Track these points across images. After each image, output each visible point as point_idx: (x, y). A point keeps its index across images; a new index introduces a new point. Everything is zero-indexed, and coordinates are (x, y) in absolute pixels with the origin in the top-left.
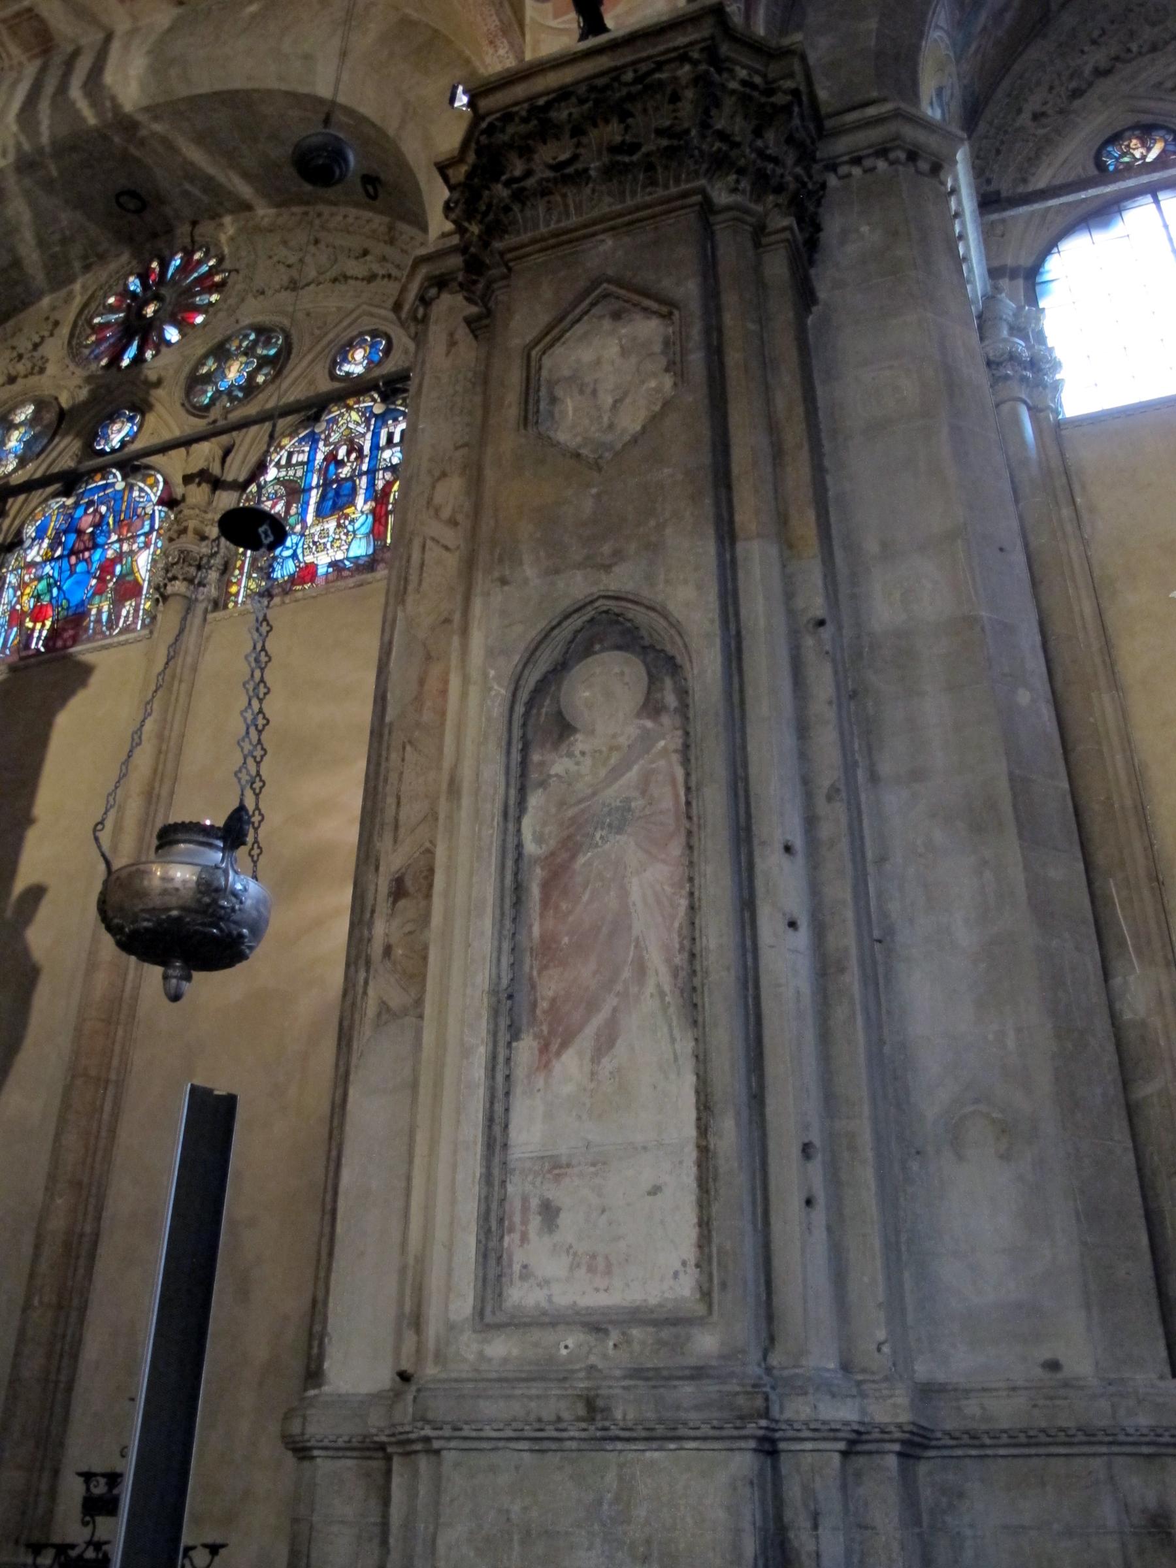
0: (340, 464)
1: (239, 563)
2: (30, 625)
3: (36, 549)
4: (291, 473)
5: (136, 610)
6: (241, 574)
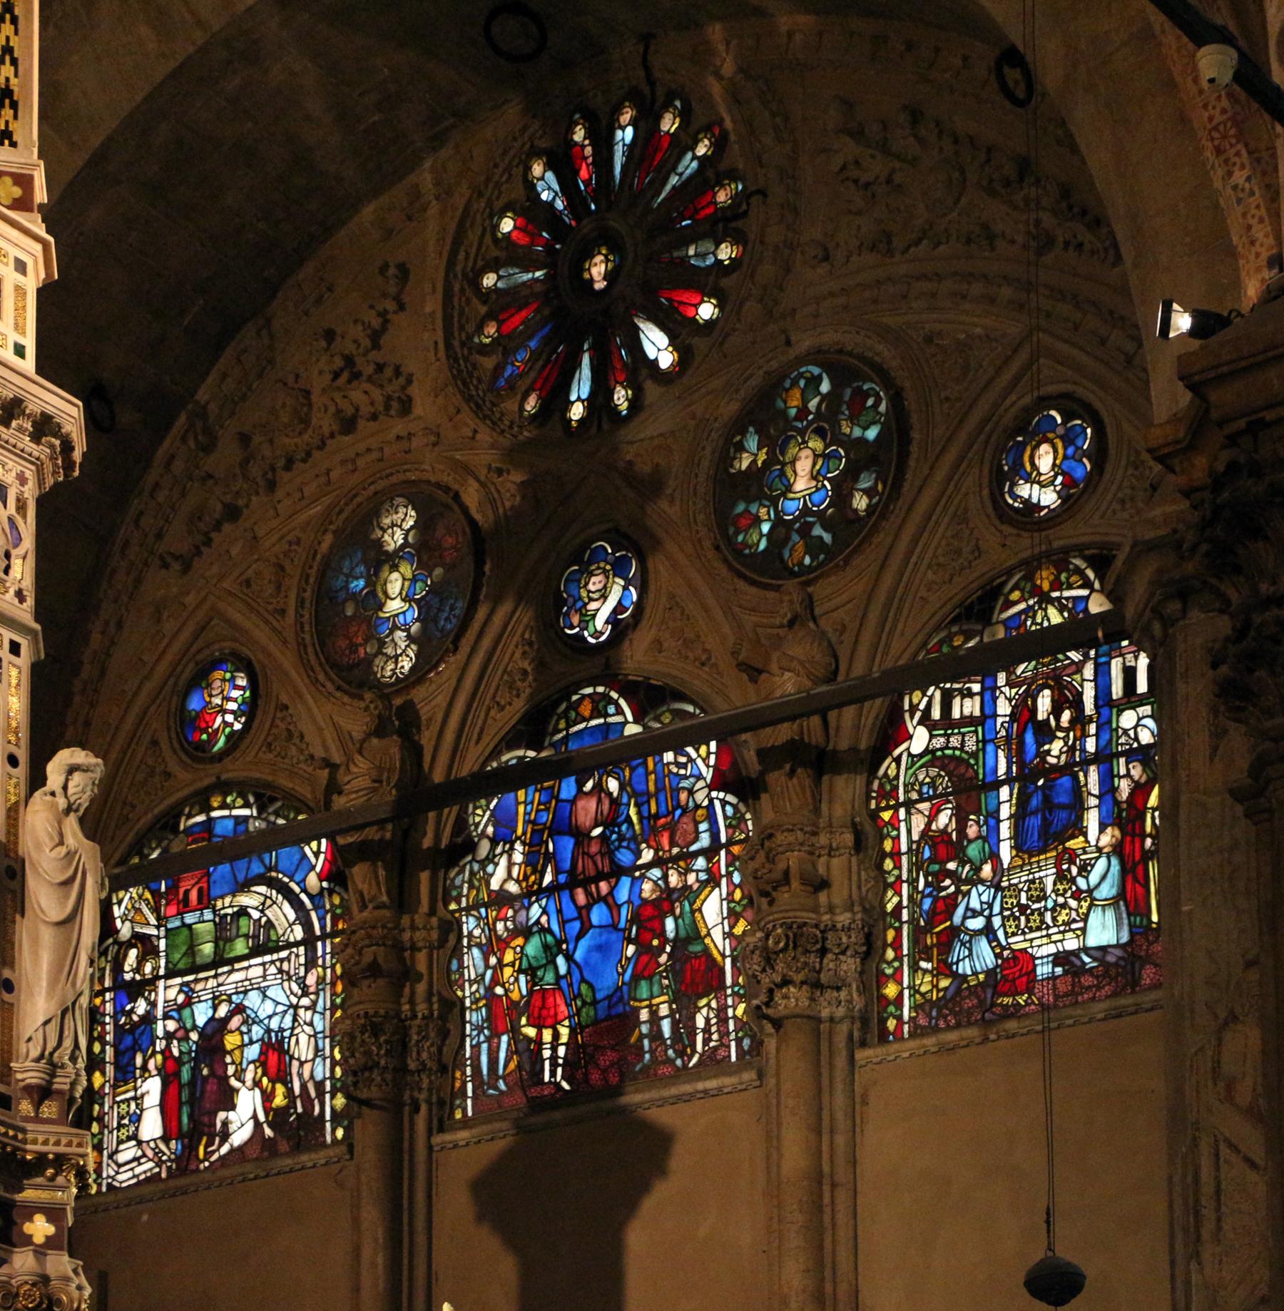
0: (1045, 733)
1: (891, 935)
2: (531, 1032)
3: (503, 861)
4: (954, 741)
5: (723, 1020)
6: (899, 957)
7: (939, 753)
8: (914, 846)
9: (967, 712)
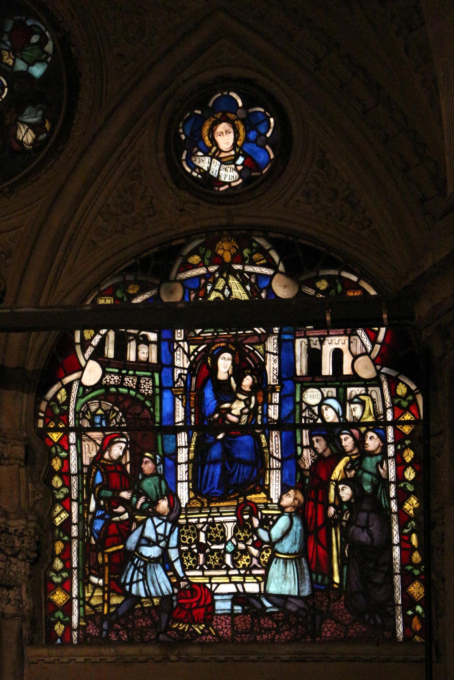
0: (225, 392)
1: (59, 547)
4: (129, 381)
6: (68, 568)
7: (113, 390)
8: (85, 470)
9: (143, 356)
